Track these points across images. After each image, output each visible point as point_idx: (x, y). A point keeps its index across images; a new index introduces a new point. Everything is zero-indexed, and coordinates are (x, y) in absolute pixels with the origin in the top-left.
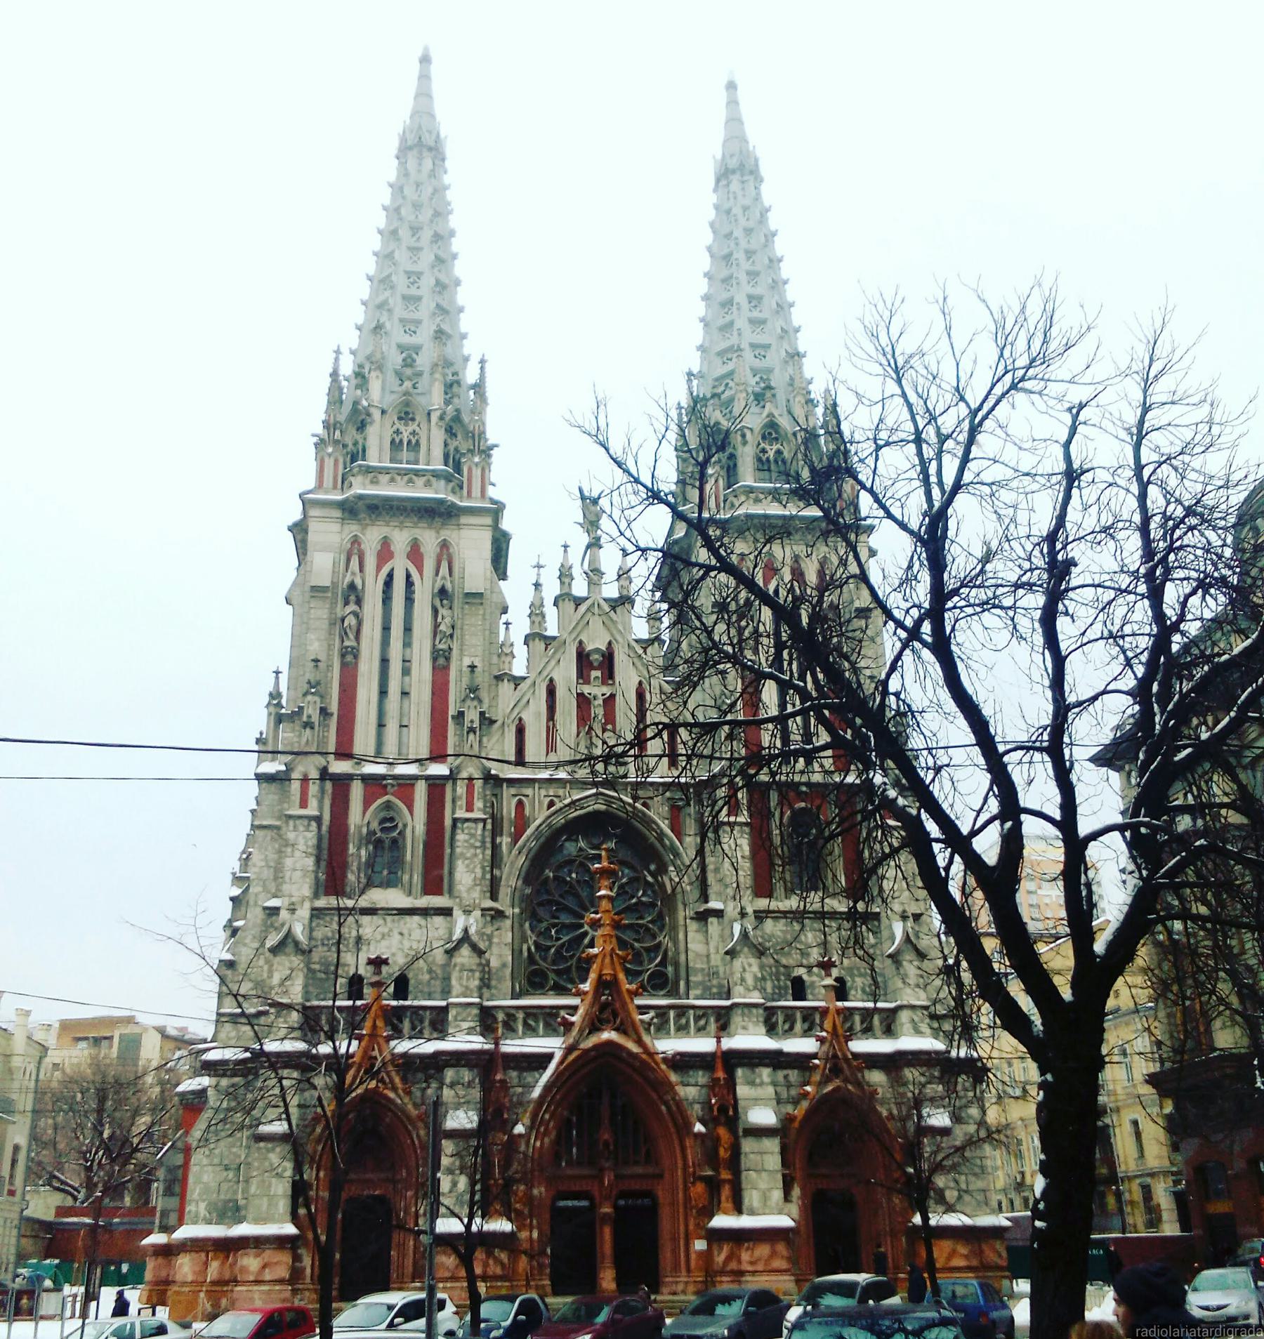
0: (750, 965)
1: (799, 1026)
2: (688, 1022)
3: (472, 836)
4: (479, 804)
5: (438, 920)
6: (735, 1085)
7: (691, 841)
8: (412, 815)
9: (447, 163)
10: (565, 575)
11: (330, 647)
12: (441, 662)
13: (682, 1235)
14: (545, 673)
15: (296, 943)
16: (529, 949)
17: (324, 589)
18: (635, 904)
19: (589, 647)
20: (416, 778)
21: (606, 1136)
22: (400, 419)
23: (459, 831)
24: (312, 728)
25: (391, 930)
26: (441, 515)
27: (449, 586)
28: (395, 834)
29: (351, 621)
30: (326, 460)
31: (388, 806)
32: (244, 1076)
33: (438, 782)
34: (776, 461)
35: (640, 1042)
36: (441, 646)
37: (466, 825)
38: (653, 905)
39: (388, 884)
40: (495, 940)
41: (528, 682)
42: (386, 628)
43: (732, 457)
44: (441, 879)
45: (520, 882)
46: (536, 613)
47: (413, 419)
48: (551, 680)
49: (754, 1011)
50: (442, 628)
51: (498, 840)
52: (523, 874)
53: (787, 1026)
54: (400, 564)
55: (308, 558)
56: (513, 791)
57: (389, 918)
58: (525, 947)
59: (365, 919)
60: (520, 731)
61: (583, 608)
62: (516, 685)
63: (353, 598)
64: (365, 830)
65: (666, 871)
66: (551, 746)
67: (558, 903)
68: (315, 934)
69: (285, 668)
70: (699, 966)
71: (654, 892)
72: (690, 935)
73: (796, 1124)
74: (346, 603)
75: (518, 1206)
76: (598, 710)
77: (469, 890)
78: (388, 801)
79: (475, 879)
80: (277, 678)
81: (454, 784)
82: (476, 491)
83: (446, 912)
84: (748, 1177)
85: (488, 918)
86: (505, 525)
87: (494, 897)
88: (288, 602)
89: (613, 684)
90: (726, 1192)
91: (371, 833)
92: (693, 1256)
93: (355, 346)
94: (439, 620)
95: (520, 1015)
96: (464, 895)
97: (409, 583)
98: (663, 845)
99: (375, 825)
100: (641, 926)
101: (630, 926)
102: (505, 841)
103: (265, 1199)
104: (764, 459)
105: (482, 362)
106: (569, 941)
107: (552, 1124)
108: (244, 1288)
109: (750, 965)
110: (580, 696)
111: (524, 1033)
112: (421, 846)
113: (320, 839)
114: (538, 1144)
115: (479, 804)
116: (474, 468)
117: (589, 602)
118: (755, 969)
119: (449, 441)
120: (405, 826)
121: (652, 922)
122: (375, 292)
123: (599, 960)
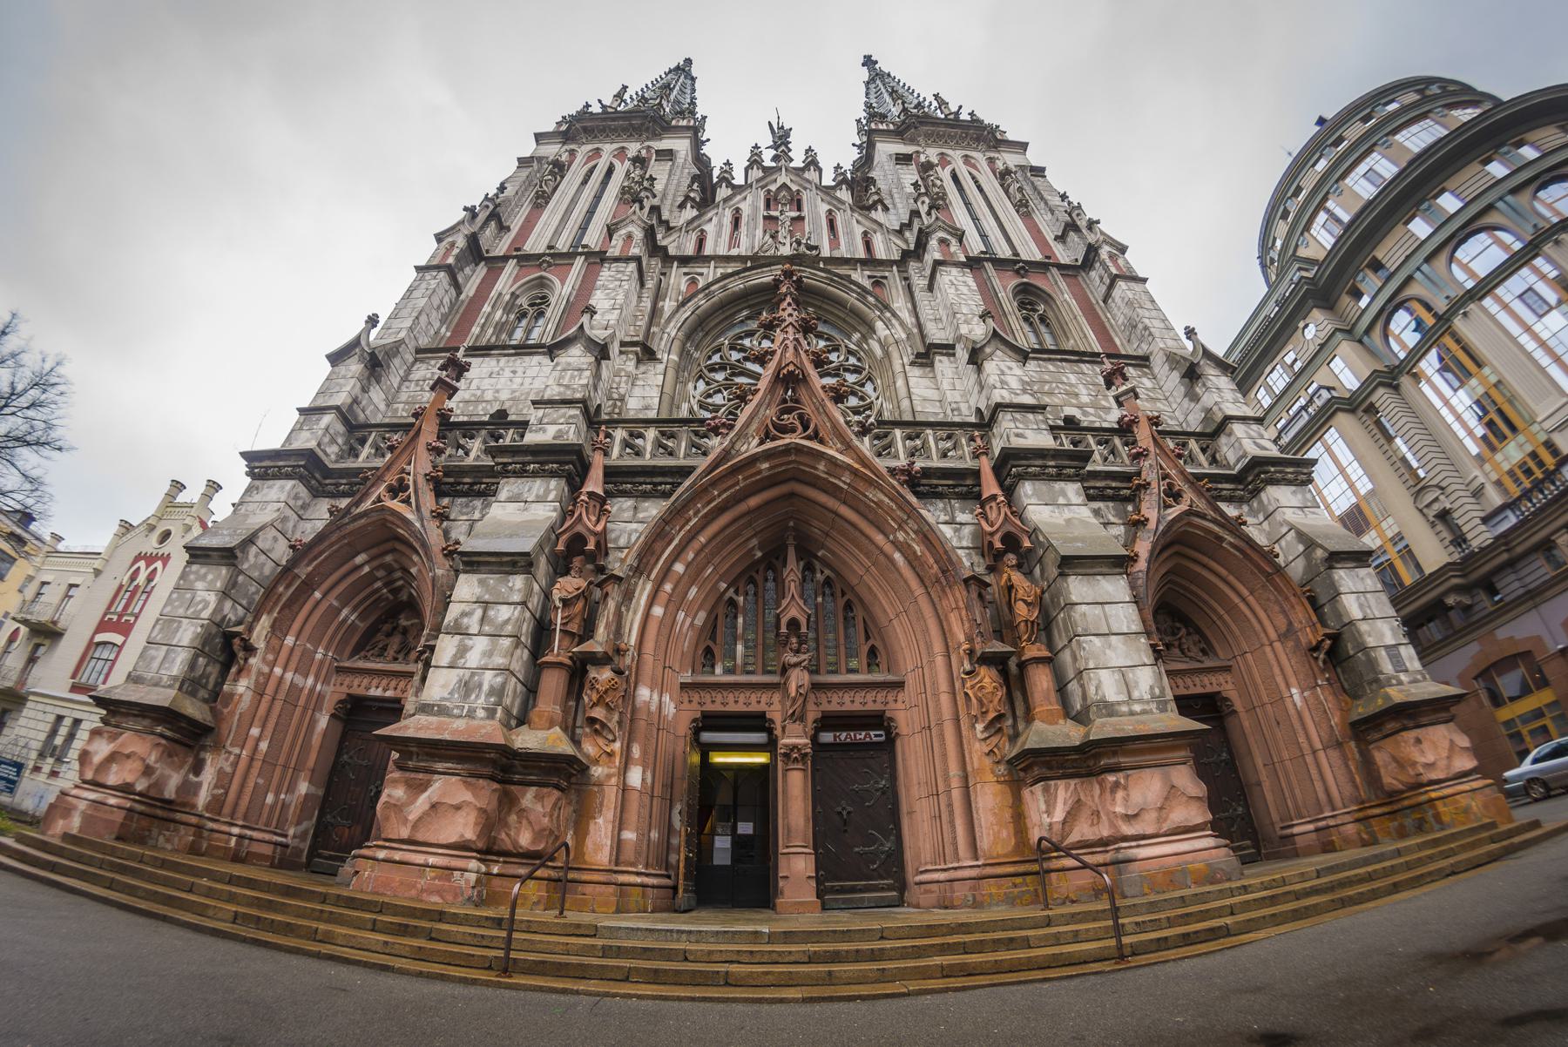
2: (925, 443)
8: (563, 284)
13: (955, 783)
21: (793, 612)
31: (542, 283)
48: (738, 210)
49: (1031, 416)
51: (661, 304)
56: (686, 270)
57: (503, 360)
64: (507, 297)
65: (872, 330)
66: (734, 241)
67: (732, 367)
71: (859, 360)
72: (912, 382)
75: (599, 713)
78: (541, 277)
85: (631, 356)
95: (651, 434)
97: (610, 171)
99: (523, 301)
102: (668, 305)
107: (693, 591)
109: (1010, 368)
111: (653, 456)
114: (658, 611)
123: (777, 357)
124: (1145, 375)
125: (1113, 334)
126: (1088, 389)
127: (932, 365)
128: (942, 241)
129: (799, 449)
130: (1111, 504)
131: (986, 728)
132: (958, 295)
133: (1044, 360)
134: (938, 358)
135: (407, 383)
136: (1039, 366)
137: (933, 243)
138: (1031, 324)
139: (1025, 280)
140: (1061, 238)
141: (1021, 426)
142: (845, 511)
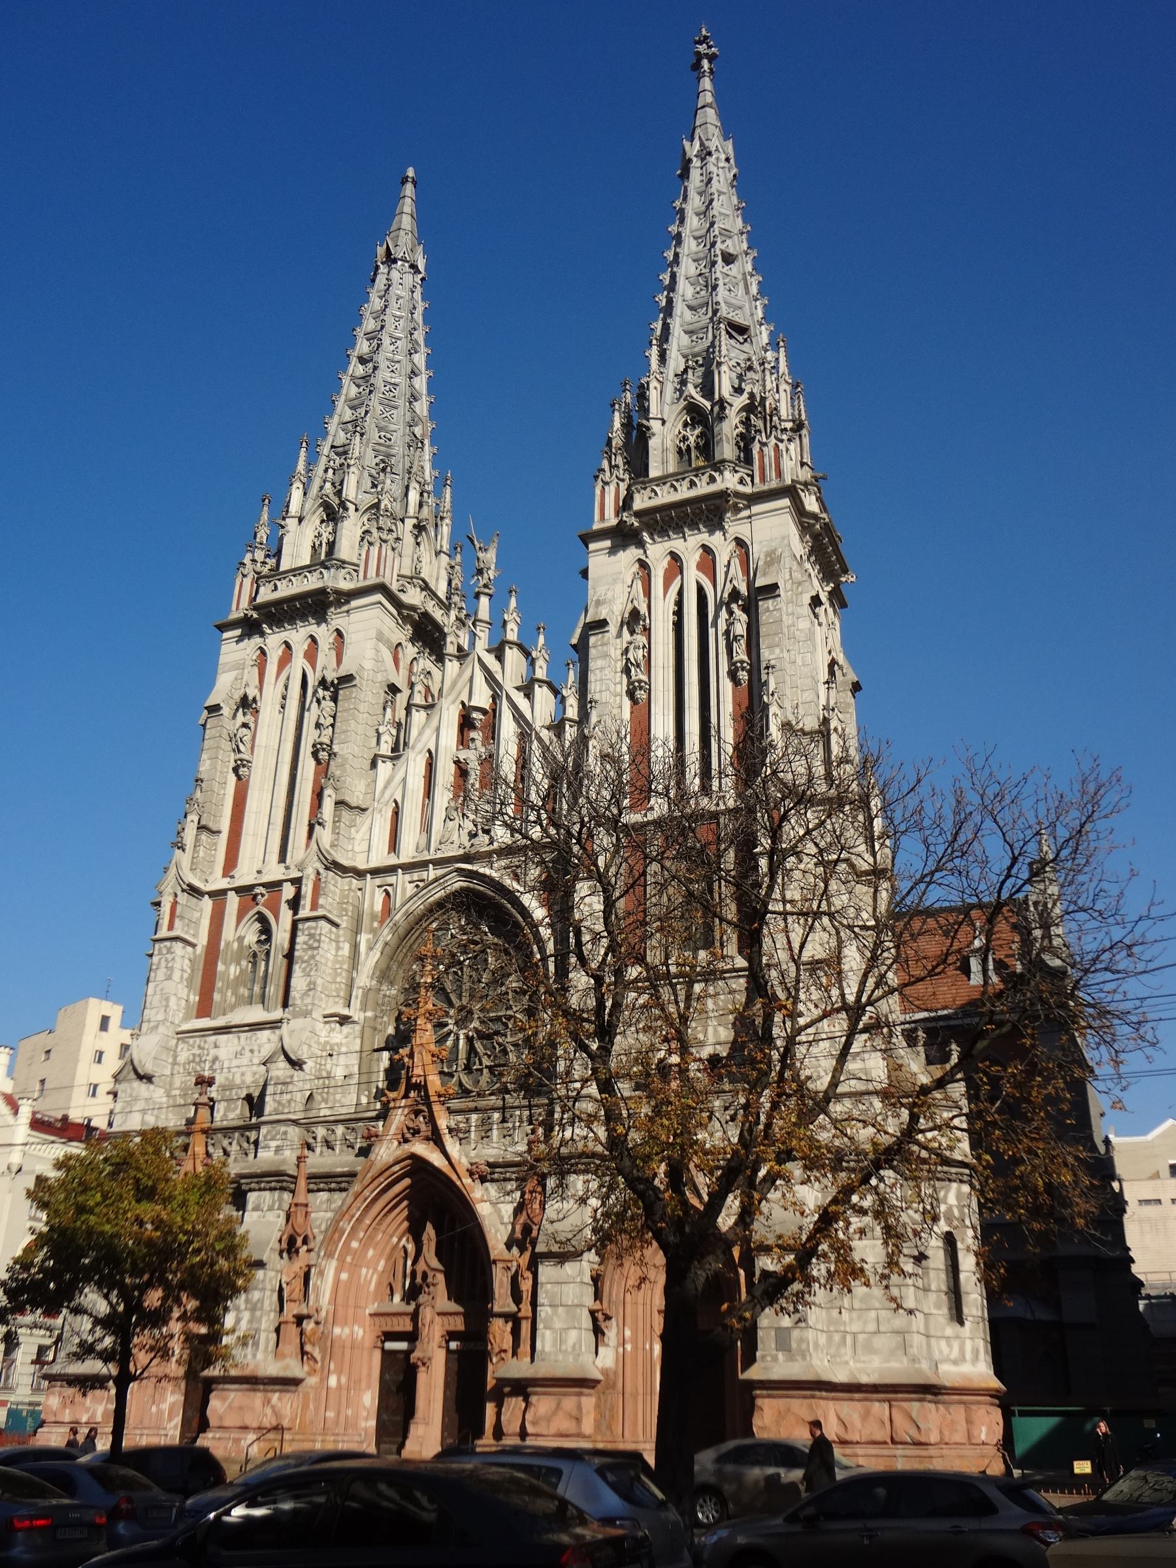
3: (311, 936)
23: (299, 933)
25: (243, 1048)
52: (377, 974)
56: (378, 881)
57: (243, 1035)
59: (223, 1038)
60: (396, 813)
64: (236, 945)
77: (302, 998)
84: (544, 1312)
96: (298, 1002)
102: (364, 939)
111: (341, 1151)
114: (344, 1276)
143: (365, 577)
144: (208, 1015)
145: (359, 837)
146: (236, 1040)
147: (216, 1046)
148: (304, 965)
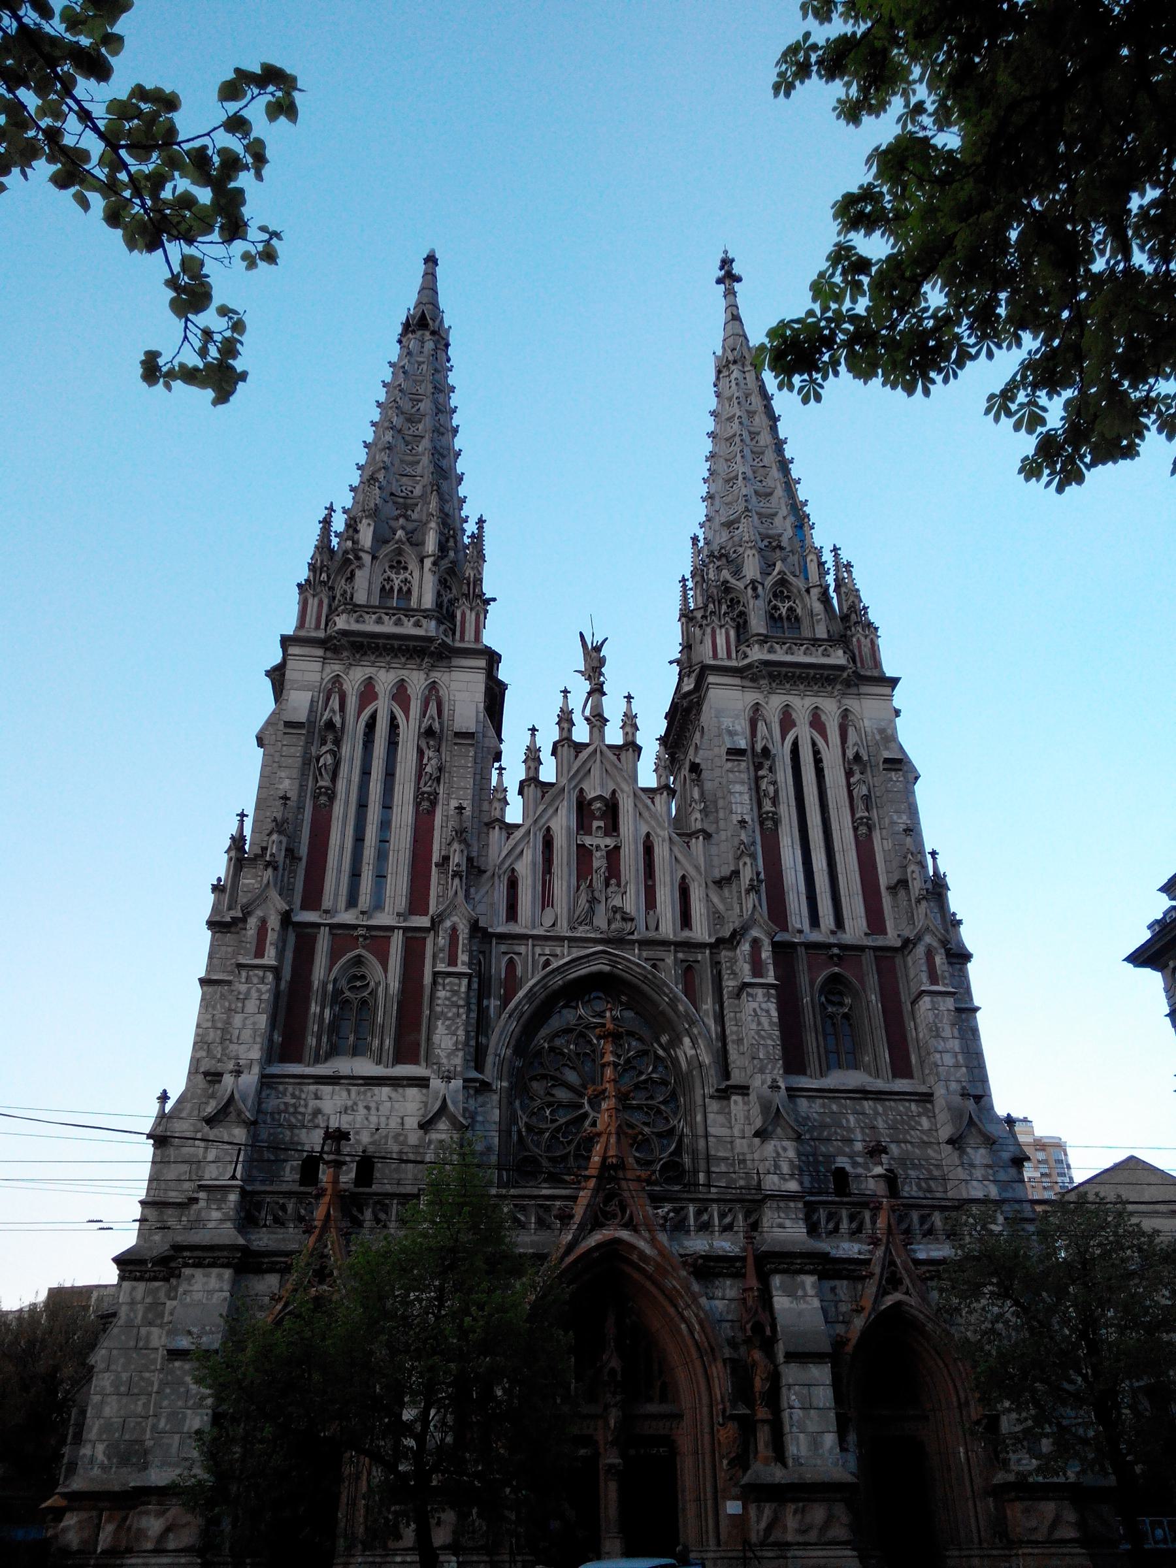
0: (785, 1149)
1: (844, 1226)
2: (711, 1217)
3: (455, 993)
4: (463, 957)
5: (412, 1092)
6: (771, 1297)
7: (708, 1005)
8: (386, 971)
9: (451, 351)
10: (565, 719)
11: (302, 787)
12: (426, 804)
14: (543, 821)
15: (239, 1113)
16: (519, 1132)
17: (298, 725)
18: (645, 1081)
19: (591, 795)
20: (392, 929)
22: (391, 567)
24: (275, 869)
25: (355, 1104)
26: (432, 654)
27: (436, 726)
28: (365, 994)
29: (329, 759)
30: (310, 601)
32: (166, 1279)
33: (418, 935)
34: (788, 618)
35: (653, 1242)
36: (426, 789)
37: (447, 980)
38: (665, 1083)
39: (356, 1052)
40: (480, 1118)
41: (522, 830)
42: (366, 773)
43: (742, 614)
44: (419, 1045)
45: (509, 1052)
46: (533, 757)
47: (406, 568)
48: (548, 829)
49: (792, 1204)
50: (428, 769)
51: (485, 1002)
52: (513, 1042)
53: (831, 1226)
54: (383, 705)
55: (284, 696)
56: (503, 948)
57: (354, 1089)
58: (515, 1128)
59: (326, 1089)
61: (584, 754)
62: (509, 835)
63: (330, 737)
64: (330, 987)
67: (553, 1078)
68: (264, 1105)
69: (250, 811)
70: (721, 1154)
71: (666, 1067)
72: (711, 1116)
73: (849, 1348)
74: (324, 743)
76: (599, 861)
77: (448, 1056)
78: (359, 956)
79: (457, 1042)
80: (242, 822)
81: (437, 935)
82: (470, 634)
83: (421, 1083)
85: (472, 1092)
86: (502, 675)
87: (479, 1067)
88: (260, 742)
89: (618, 836)
90: (763, 1435)
91: (337, 992)
92: (723, 1523)
93: (349, 505)
94: (425, 761)
96: (444, 1061)
97: (394, 726)
98: (676, 1011)
99: (343, 983)
100: (650, 1107)
101: (639, 1107)
102: (493, 1003)
103: (177, 1437)
104: (776, 615)
105: (481, 522)
106: (567, 1124)
108: (140, 1561)
110: (581, 847)
112: (395, 1007)
113: (277, 995)
115: (463, 957)
116: (468, 612)
117: (590, 749)
118: (791, 1154)
119: (443, 592)
120: (378, 984)
121: (664, 1102)
122: (371, 458)
123: (603, 1139)
124: (925, 1113)
125: (911, 1050)
126: (863, 1133)
127: (728, 1098)
128: (756, 943)
129: (618, 1241)
130: (845, 1282)
131: (728, 1464)
132: (758, 1032)
133: (826, 1097)
134: (734, 1098)
135: (261, 1116)
136: (824, 1106)
137: (746, 947)
138: (834, 1024)
139: (836, 969)
140: (892, 889)
141: (782, 1215)
142: (648, 1284)
143: (462, 639)
144: (299, 1060)
145: (477, 898)
146: (345, 1094)
147: (317, 1097)
148: (447, 1023)
